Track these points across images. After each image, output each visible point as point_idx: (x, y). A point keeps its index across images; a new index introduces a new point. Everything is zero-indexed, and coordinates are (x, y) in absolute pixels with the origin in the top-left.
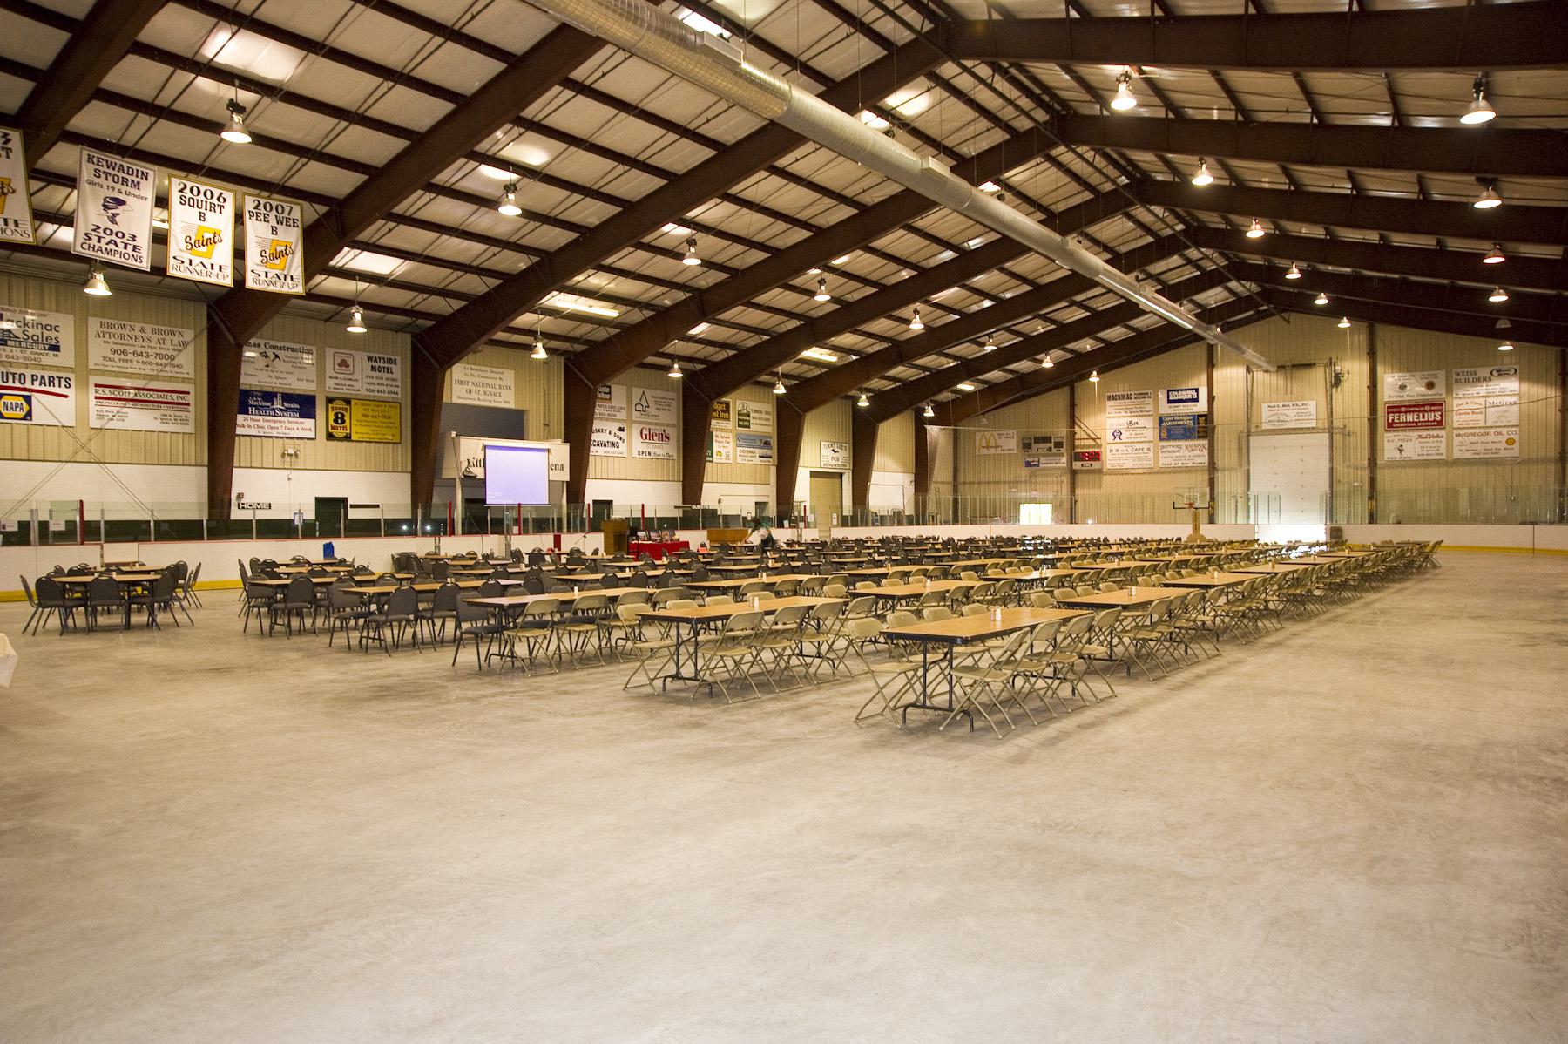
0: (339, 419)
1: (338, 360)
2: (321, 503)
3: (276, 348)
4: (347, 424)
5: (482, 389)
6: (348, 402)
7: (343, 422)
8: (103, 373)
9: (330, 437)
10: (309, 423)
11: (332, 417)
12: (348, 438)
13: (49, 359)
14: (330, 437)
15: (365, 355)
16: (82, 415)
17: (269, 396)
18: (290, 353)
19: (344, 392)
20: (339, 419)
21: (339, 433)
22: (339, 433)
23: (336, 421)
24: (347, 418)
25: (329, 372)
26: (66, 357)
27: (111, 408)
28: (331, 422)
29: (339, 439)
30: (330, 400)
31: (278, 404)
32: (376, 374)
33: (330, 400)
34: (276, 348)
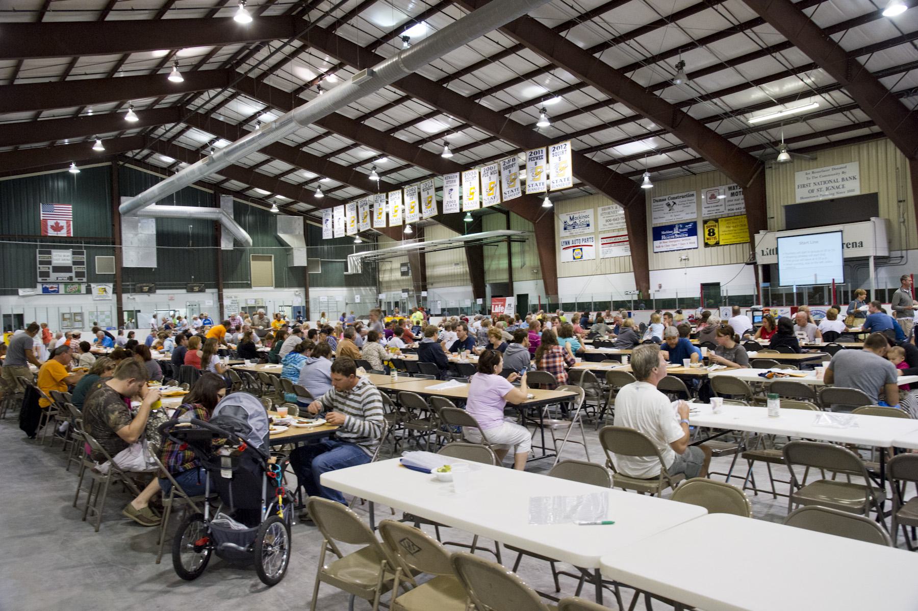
0: (712, 233)
1: (709, 195)
2: (704, 286)
3: (674, 198)
4: (717, 235)
5: (824, 186)
6: (716, 220)
7: (714, 234)
8: (604, 232)
9: (706, 245)
10: (694, 238)
11: (707, 232)
12: (717, 244)
13: (587, 230)
14: (706, 245)
15: (726, 187)
16: (597, 253)
17: (671, 227)
18: (682, 199)
19: (714, 215)
20: (712, 233)
21: (712, 242)
22: (712, 242)
23: (709, 235)
24: (716, 231)
25: (704, 205)
26: (591, 229)
27: (607, 248)
28: (707, 236)
29: (712, 246)
30: (705, 222)
31: (676, 231)
32: (736, 197)
33: (705, 222)
34: (674, 198)
